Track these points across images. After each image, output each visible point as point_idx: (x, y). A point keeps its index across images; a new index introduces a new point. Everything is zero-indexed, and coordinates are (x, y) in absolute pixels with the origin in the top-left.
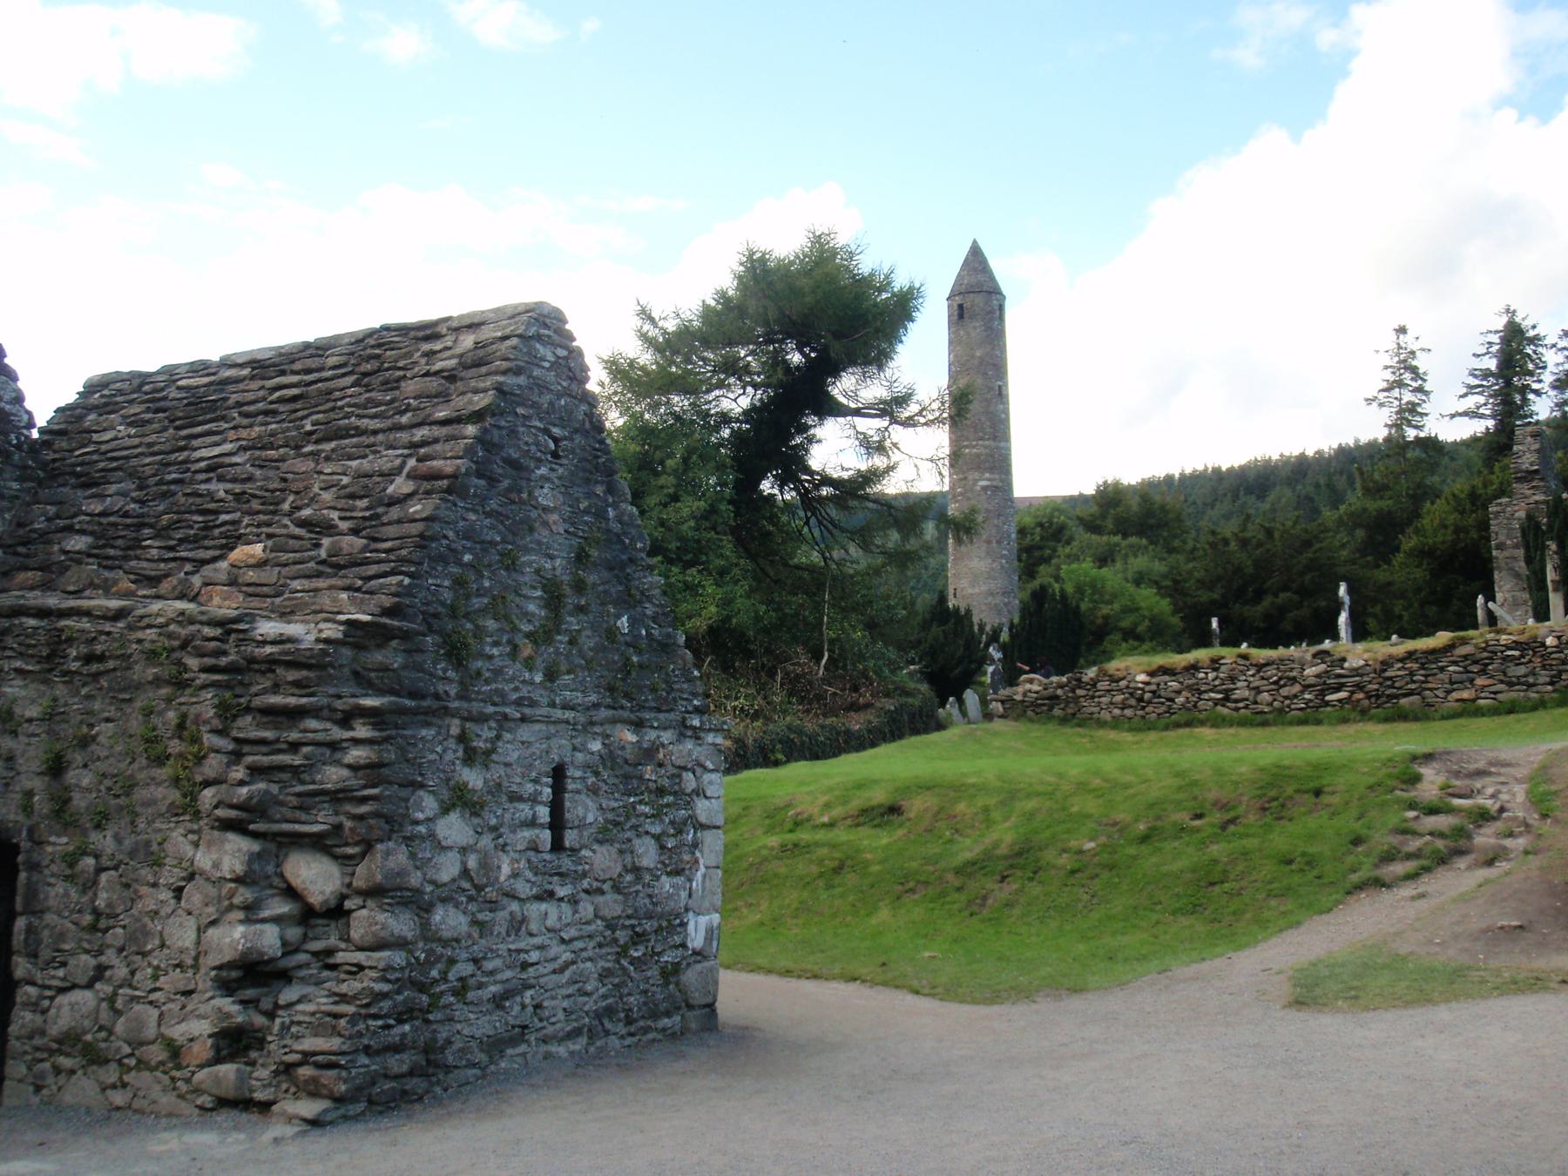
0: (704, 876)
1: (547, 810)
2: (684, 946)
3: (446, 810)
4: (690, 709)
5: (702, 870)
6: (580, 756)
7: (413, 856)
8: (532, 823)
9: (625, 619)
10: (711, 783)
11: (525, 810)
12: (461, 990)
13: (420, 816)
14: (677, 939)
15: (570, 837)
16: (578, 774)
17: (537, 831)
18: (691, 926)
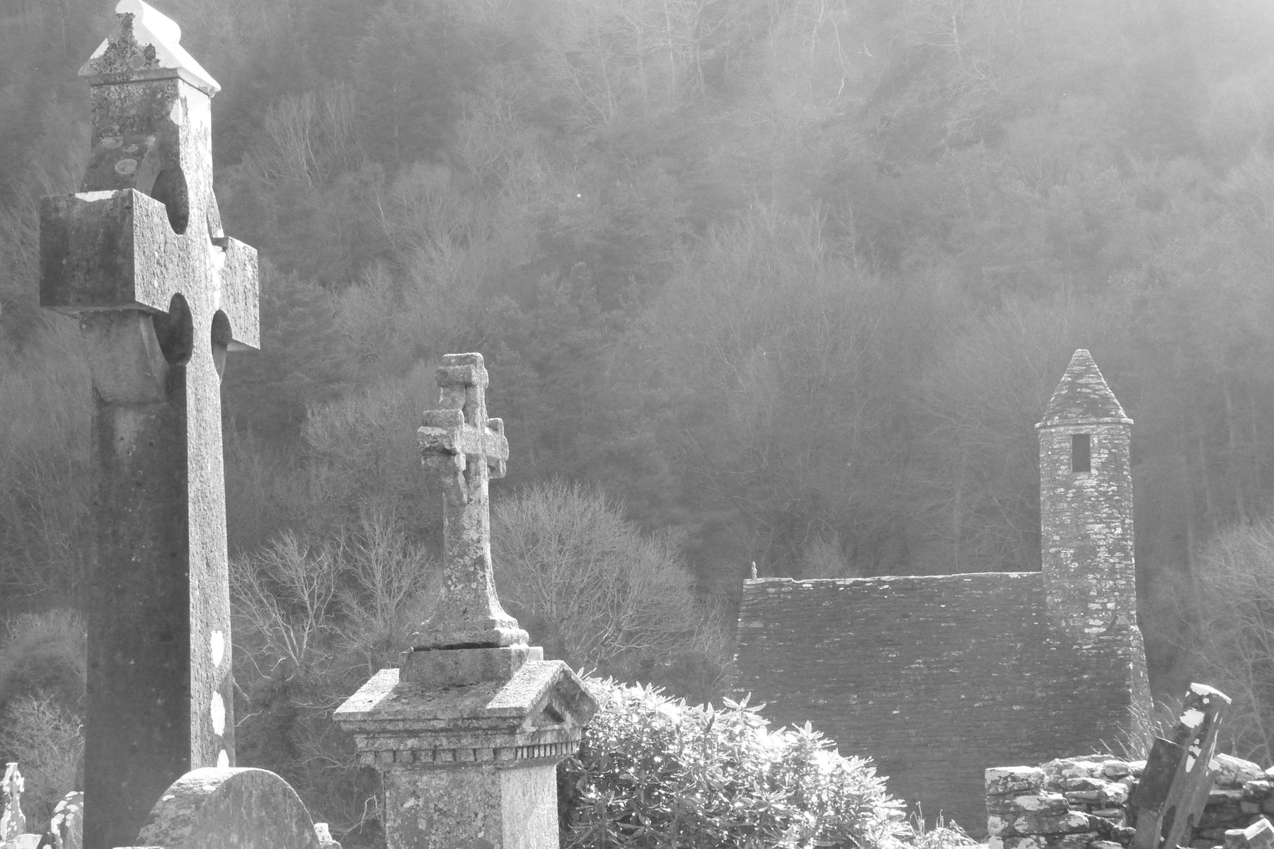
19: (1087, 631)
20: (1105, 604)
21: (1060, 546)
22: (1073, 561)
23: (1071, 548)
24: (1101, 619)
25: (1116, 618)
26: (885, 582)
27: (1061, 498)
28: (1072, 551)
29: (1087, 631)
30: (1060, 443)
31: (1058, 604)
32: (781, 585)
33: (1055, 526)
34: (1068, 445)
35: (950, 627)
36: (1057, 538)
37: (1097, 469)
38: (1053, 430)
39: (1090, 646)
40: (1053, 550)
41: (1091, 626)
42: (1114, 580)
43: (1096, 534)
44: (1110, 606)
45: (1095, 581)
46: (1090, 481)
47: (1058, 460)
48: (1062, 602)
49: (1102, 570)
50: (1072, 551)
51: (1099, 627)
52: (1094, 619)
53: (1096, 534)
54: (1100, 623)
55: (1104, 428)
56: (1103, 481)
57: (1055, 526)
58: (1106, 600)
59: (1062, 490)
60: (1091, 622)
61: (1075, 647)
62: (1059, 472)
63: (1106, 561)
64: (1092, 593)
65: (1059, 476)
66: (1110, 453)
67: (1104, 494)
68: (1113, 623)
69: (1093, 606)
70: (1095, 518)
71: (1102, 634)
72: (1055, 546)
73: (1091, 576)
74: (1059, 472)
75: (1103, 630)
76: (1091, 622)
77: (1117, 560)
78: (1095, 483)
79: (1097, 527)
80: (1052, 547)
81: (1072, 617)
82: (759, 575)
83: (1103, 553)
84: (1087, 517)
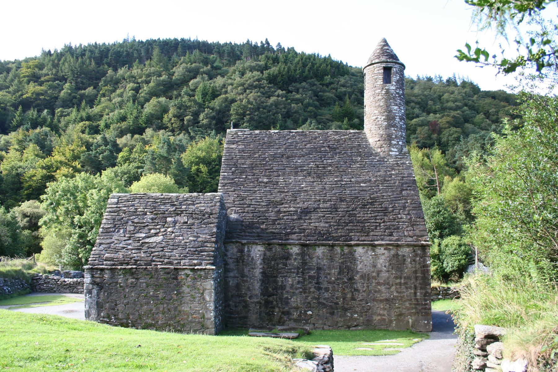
19: (391, 153)
20: (398, 142)
24: (396, 148)
25: (402, 149)
26: (293, 132)
28: (384, 117)
29: (391, 153)
32: (245, 131)
34: (382, 71)
35: (326, 150)
37: (395, 82)
39: (392, 160)
40: (375, 117)
41: (393, 151)
42: (402, 132)
43: (395, 110)
44: (400, 143)
45: (394, 131)
46: (392, 87)
48: (379, 141)
49: (397, 127)
50: (384, 117)
51: (396, 152)
52: (394, 148)
53: (395, 110)
54: (396, 150)
55: (397, 66)
56: (397, 88)
58: (399, 140)
59: (380, 91)
60: (393, 149)
61: (386, 160)
63: (399, 123)
64: (393, 137)
66: (400, 77)
67: (398, 93)
68: (402, 151)
69: (394, 142)
70: (394, 103)
71: (397, 155)
73: (393, 129)
75: (397, 153)
76: (393, 149)
77: (402, 124)
78: (394, 88)
79: (396, 107)
82: (234, 128)
83: (397, 119)
84: (391, 102)
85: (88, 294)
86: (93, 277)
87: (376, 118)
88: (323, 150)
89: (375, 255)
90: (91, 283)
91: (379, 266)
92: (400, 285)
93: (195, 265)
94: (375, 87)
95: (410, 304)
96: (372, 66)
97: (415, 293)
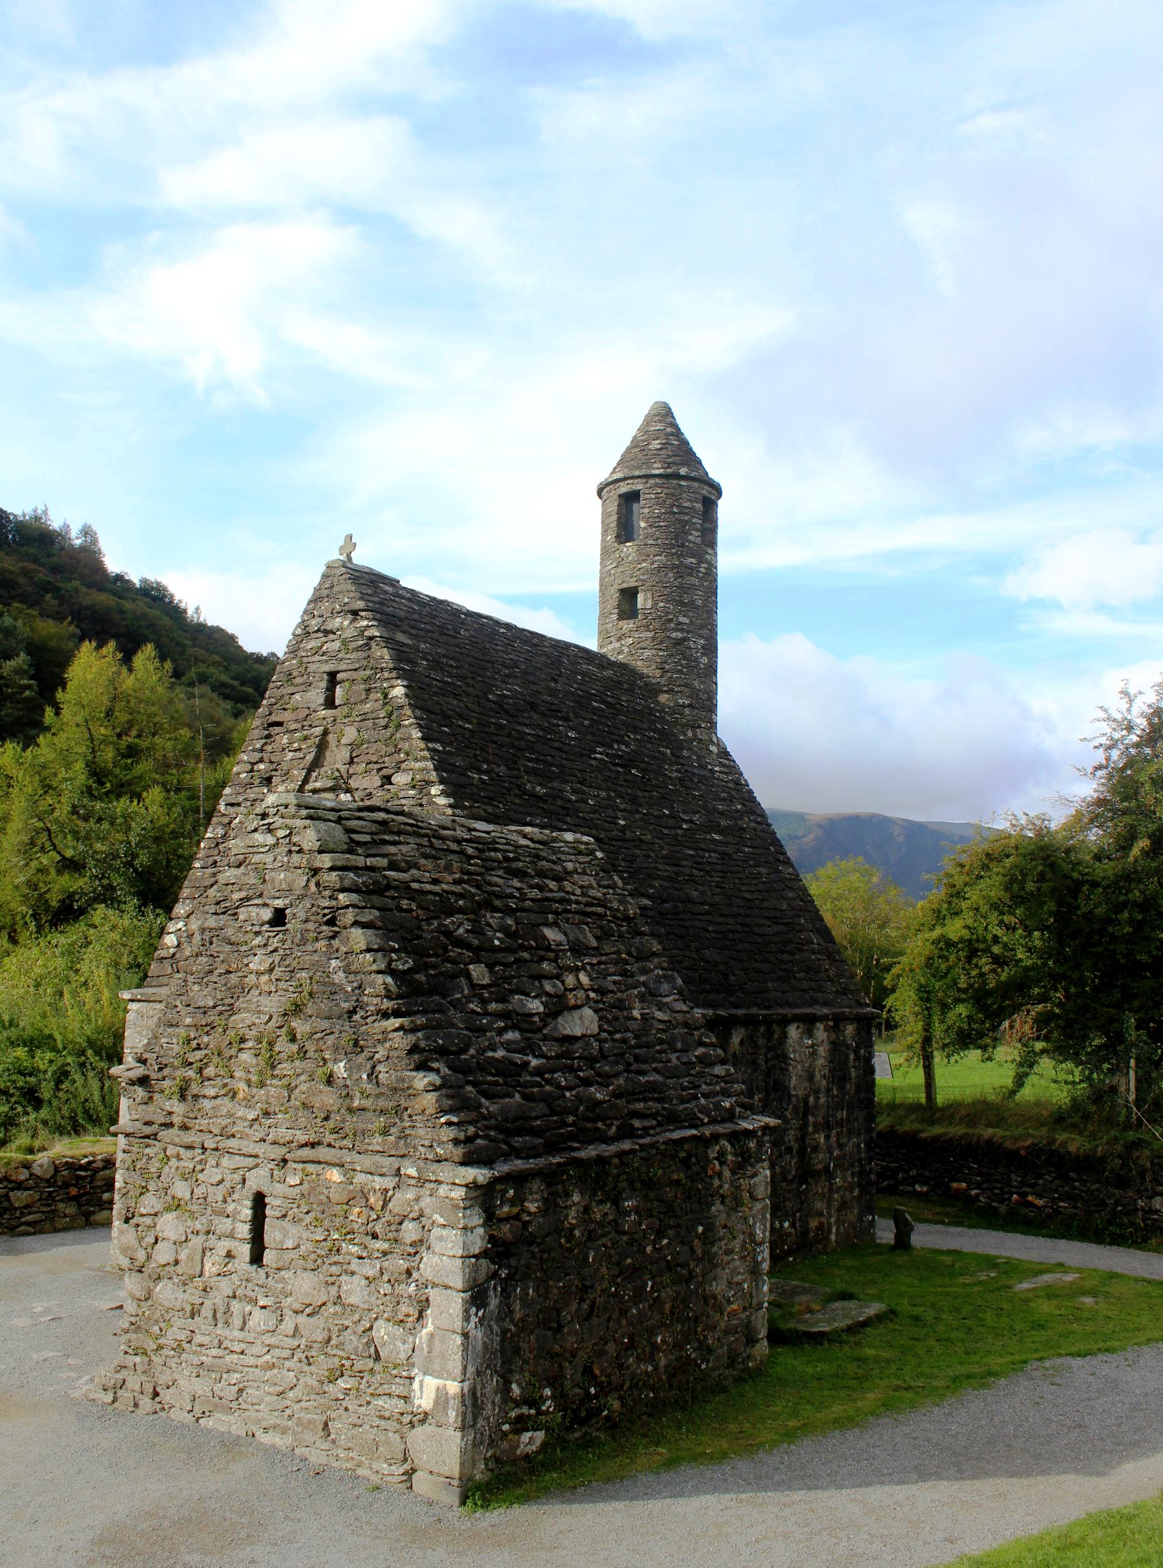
0: (431, 1336)
1: (247, 1227)
2: (406, 1398)
3: (168, 1209)
4: (431, 1157)
5: (430, 1328)
6: (279, 1188)
7: (140, 1240)
8: (231, 1236)
9: (342, 1064)
10: (440, 1238)
11: (225, 1225)
12: (179, 1348)
13: (143, 1211)
14: (396, 1390)
15: (268, 1257)
16: (278, 1202)
17: (237, 1244)
18: (416, 1385)
21: (688, 632)
22: (704, 654)
23: (702, 637)
27: (691, 570)
28: (702, 641)
30: (691, 501)
31: (683, 706)
33: (682, 604)
34: (699, 506)
36: (682, 619)
38: (683, 483)
40: (679, 635)
47: (687, 522)
48: (690, 705)
57: (682, 604)
59: (694, 561)
62: (690, 537)
65: (690, 542)
72: (681, 630)
74: (690, 537)
80: (675, 630)
81: (699, 727)
85: (474, 1309)
86: (490, 1217)
87: (684, 639)
88: (594, 708)
89: (812, 1046)
90: (484, 1254)
91: (818, 1077)
92: (842, 1126)
93: (730, 1116)
94: (683, 546)
95: (853, 1174)
96: (674, 482)
97: (859, 1144)
